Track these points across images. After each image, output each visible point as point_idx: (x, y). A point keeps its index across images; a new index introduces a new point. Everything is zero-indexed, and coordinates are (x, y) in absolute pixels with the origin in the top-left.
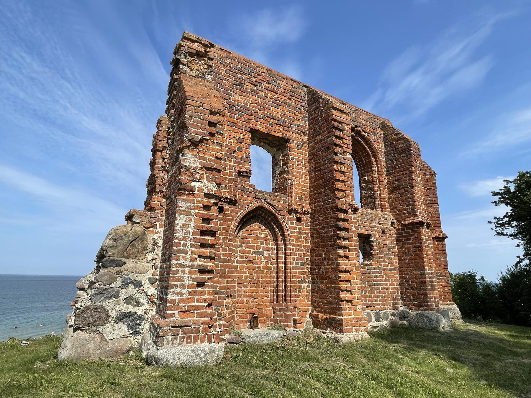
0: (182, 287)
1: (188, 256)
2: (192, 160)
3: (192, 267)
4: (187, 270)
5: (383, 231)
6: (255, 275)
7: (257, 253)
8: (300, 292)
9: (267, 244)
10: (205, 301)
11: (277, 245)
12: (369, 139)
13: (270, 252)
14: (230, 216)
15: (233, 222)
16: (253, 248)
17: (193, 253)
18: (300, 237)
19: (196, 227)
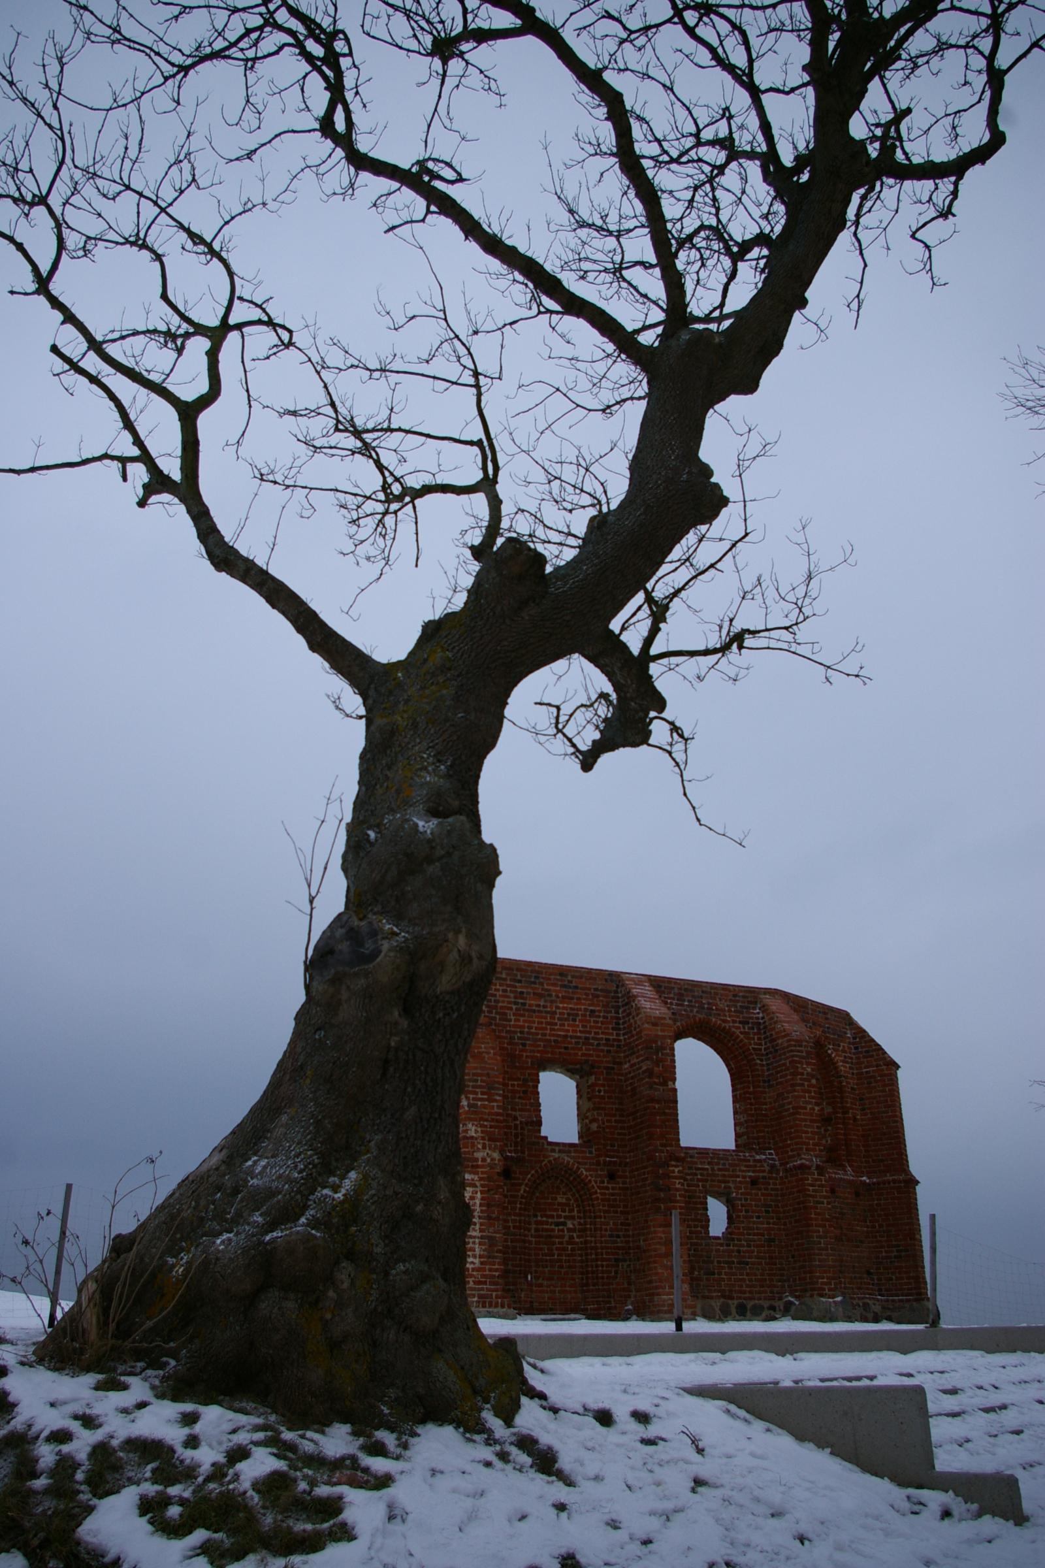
0: (474, 1256)
1: (477, 1227)
2: (474, 1128)
3: (482, 1237)
4: (477, 1241)
5: (754, 1182)
6: (556, 1252)
7: (557, 1224)
8: (616, 1272)
9: (571, 1211)
10: (496, 1270)
11: (585, 1212)
12: (734, 1033)
13: (575, 1222)
14: (519, 1179)
15: (523, 1187)
16: (552, 1217)
17: (481, 1224)
18: (615, 1200)
19: (482, 1199)
